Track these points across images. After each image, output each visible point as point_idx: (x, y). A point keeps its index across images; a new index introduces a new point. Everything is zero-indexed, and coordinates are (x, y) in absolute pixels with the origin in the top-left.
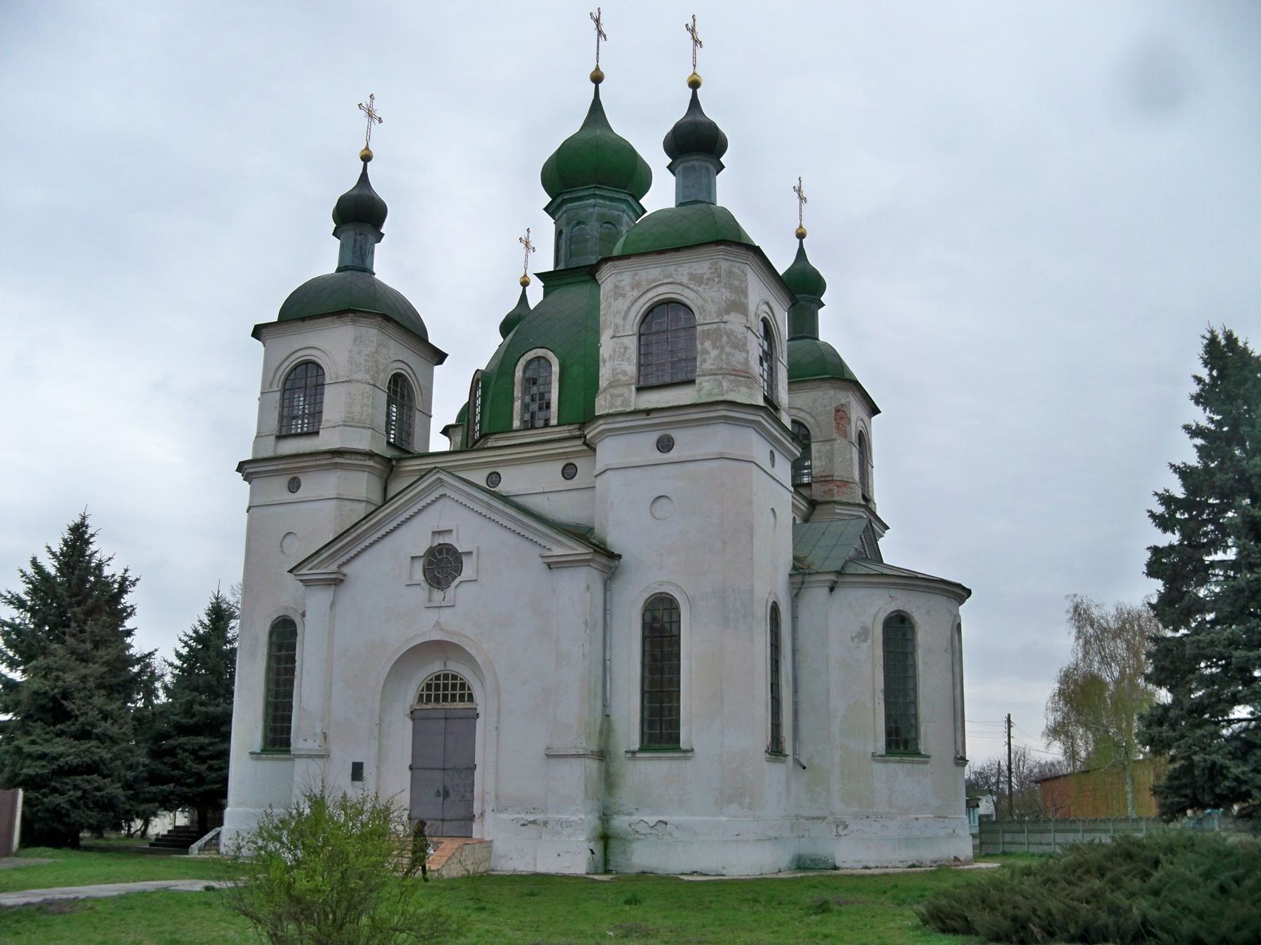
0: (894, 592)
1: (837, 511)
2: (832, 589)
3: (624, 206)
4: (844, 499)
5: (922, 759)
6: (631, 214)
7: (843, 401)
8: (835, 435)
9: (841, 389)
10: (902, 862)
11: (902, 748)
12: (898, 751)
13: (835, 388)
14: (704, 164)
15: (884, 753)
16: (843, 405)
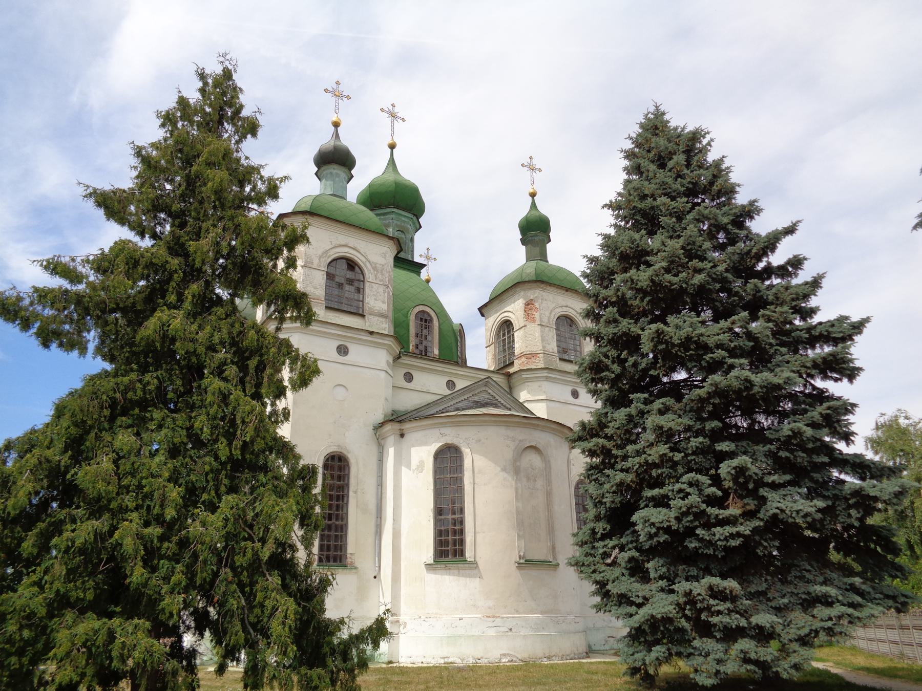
0: (444, 430)
1: (523, 376)
2: (402, 436)
3: (393, 216)
4: (533, 367)
5: (467, 565)
6: (403, 219)
7: (532, 298)
8: (527, 323)
9: (530, 289)
10: (444, 658)
11: (450, 557)
12: (447, 559)
13: (524, 290)
14: (328, 171)
15: (432, 562)
16: (532, 300)
